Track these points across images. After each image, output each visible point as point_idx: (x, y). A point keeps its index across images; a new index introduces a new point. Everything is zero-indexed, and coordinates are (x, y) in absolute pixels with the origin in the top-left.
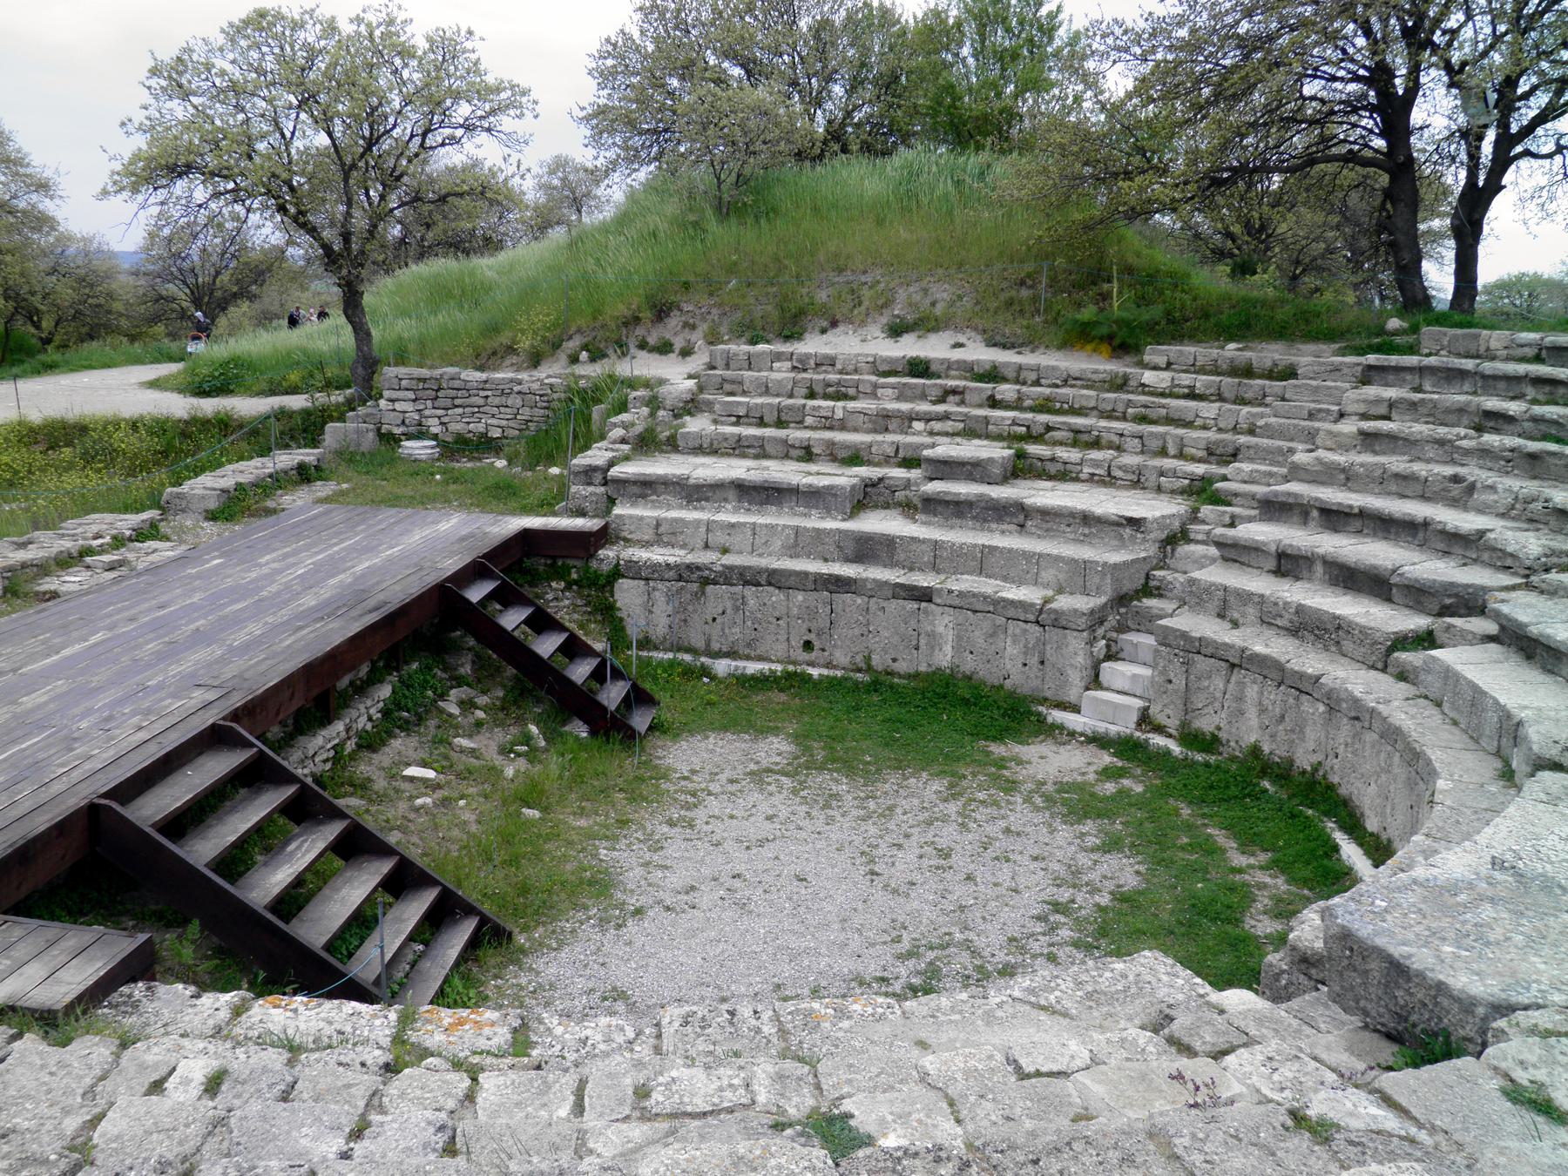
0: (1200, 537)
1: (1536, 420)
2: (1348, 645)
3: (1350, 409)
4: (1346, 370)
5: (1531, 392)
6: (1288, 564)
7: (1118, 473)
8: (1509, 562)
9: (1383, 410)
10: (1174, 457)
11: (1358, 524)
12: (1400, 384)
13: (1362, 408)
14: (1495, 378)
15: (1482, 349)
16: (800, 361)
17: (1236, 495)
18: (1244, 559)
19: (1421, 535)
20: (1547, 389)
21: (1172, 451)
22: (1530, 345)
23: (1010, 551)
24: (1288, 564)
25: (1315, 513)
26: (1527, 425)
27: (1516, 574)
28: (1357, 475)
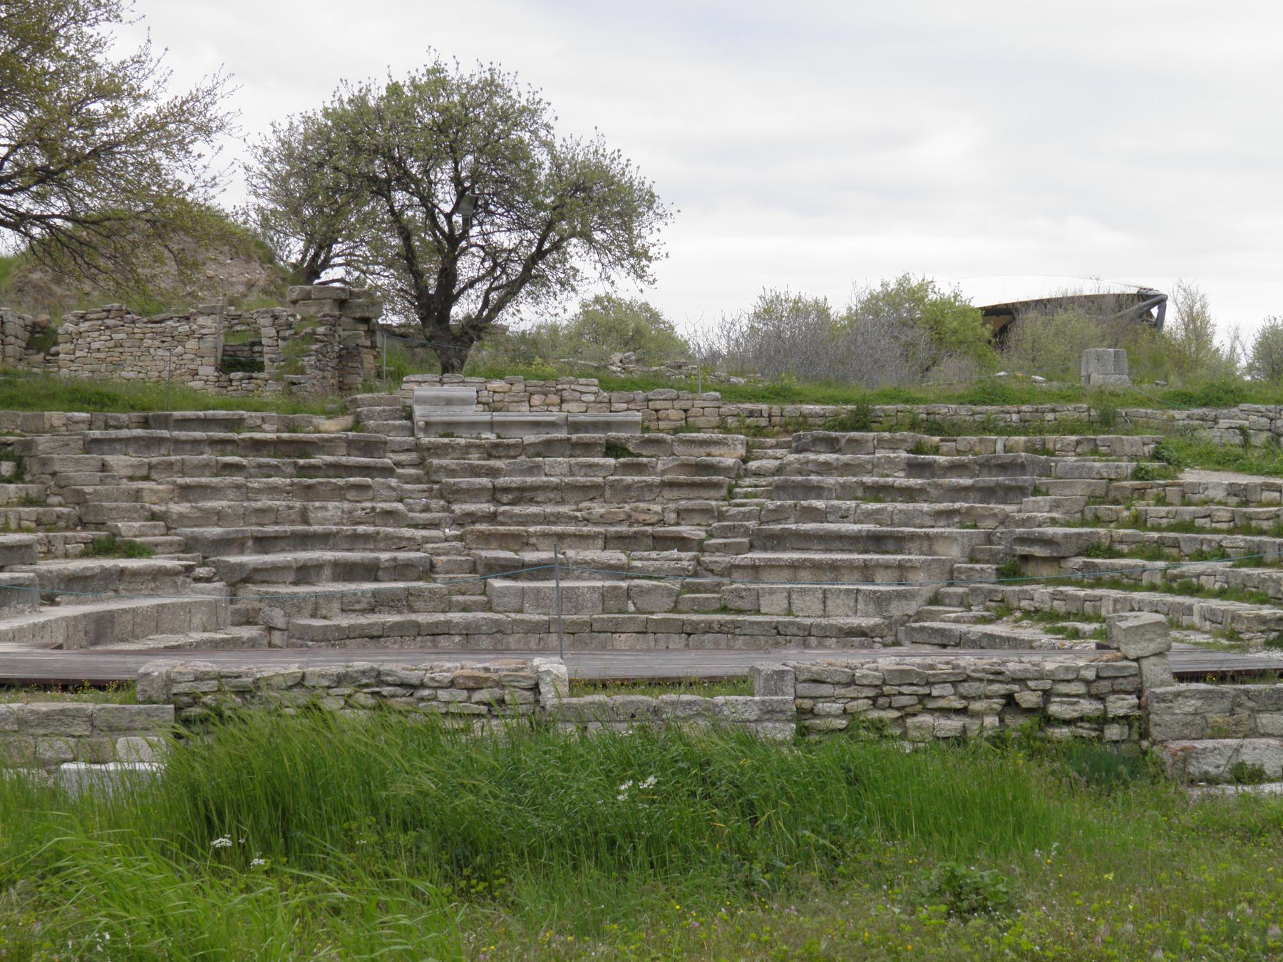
2: (419, 604)
4: (73, 445)
5: (207, 449)
6: (305, 573)
8: (404, 544)
9: (144, 472)
10: (15, 531)
13: (129, 472)
15: (47, 426)
17: (156, 545)
18: (273, 578)
19: (331, 542)
20: (219, 447)
21: (13, 525)
22: (83, 422)
23: (173, 604)
24: (305, 573)
25: (250, 543)
26: (252, 471)
28: (228, 515)
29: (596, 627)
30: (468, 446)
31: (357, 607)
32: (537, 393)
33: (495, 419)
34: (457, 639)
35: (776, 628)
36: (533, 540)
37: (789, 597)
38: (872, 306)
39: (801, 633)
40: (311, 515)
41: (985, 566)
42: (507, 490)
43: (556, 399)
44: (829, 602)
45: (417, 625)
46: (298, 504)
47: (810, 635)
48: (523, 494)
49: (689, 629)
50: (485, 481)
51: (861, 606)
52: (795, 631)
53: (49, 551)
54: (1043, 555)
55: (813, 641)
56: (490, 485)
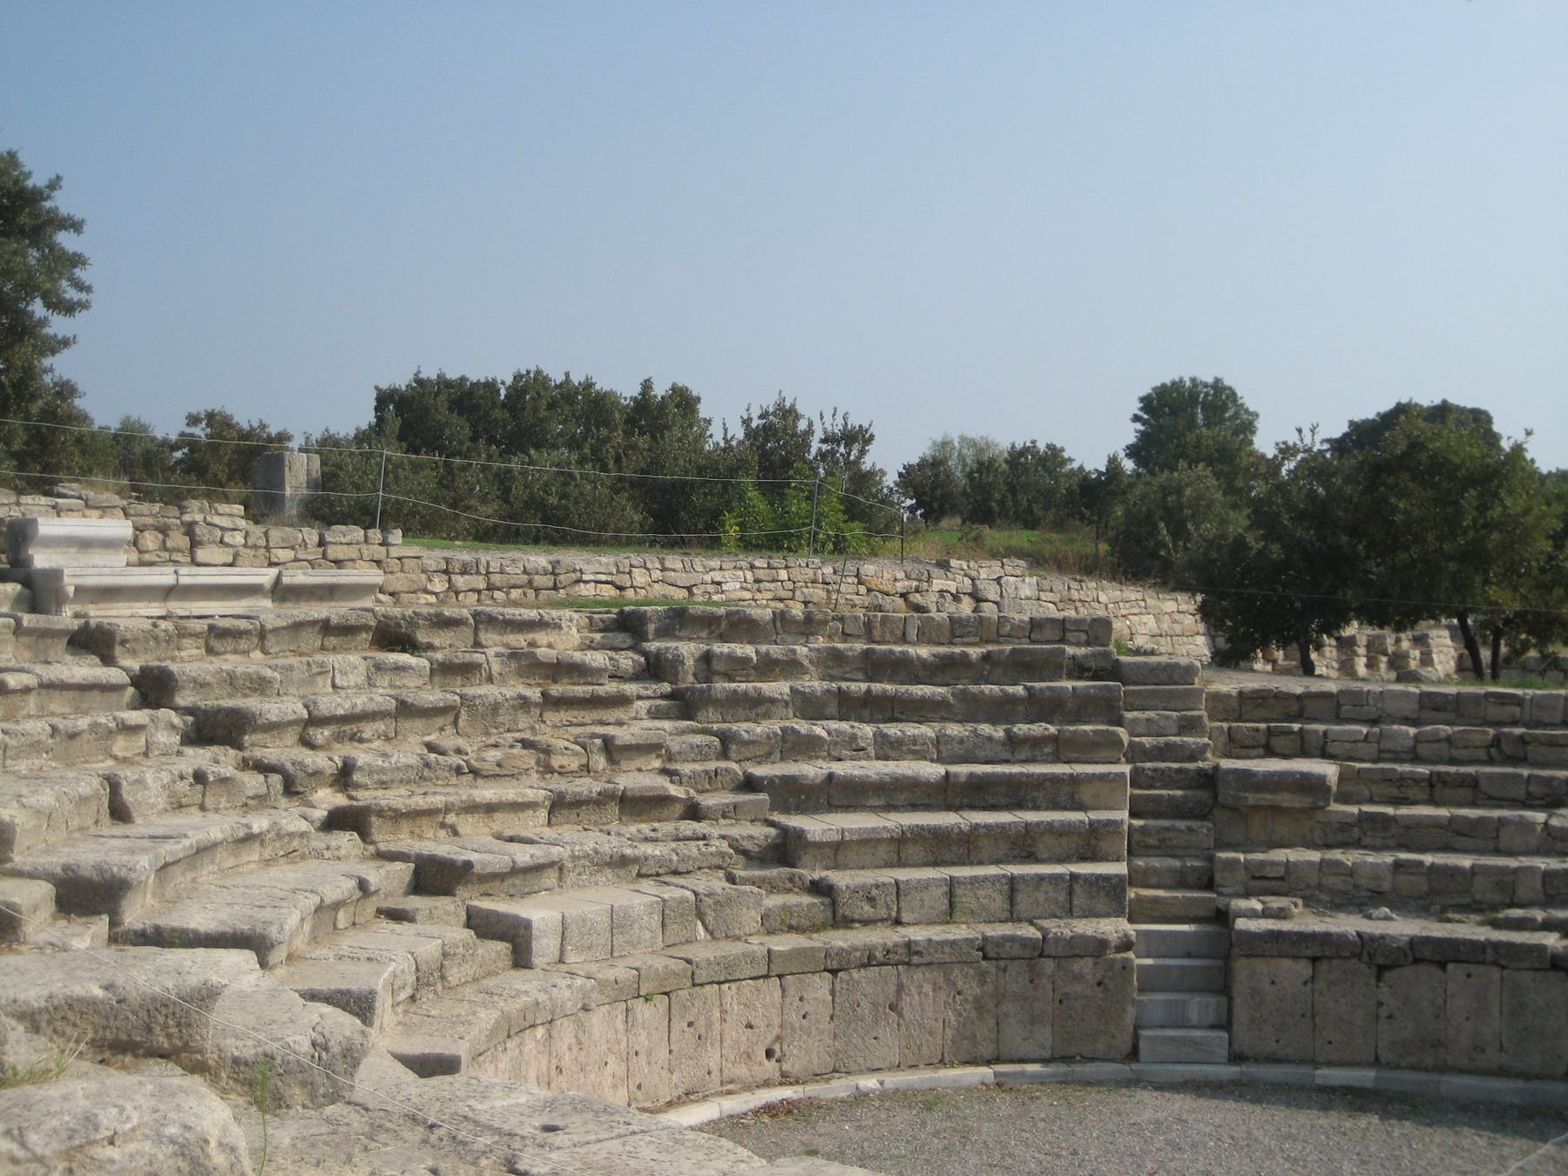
35: (981, 949)
36: (451, 818)
37: (951, 894)
39: (1027, 954)
40: (127, 795)
41: (1194, 824)
44: (1020, 897)
47: (1041, 956)
48: (349, 724)
49: (835, 965)
51: (1080, 900)
52: (1016, 950)
54: (1298, 805)
55: (1048, 965)
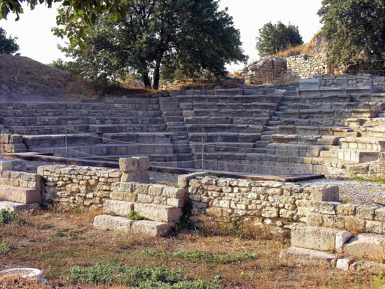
0: (175, 139)
1: (230, 105)
3: (183, 108)
5: (220, 100)
6: (210, 139)
7: (137, 128)
9: (191, 107)
11: (215, 129)
12: (187, 102)
14: (212, 98)
16: (15, 106)
19: (232, 129)
24: (210, 139)
25: (203, 129)
27: (259, 133)
29: (290, 160)
30: (306, 99)
31: (221, 149)
32: (350, 80)
33: (321, 89)
34: (248, 161)
38: (26, 58)
42: (304, 113)
43: (355, 82)
45: (234, 156)
46: (231, 118)
50: (297, 111)
53: (142, 130)
56: (298, 112)
